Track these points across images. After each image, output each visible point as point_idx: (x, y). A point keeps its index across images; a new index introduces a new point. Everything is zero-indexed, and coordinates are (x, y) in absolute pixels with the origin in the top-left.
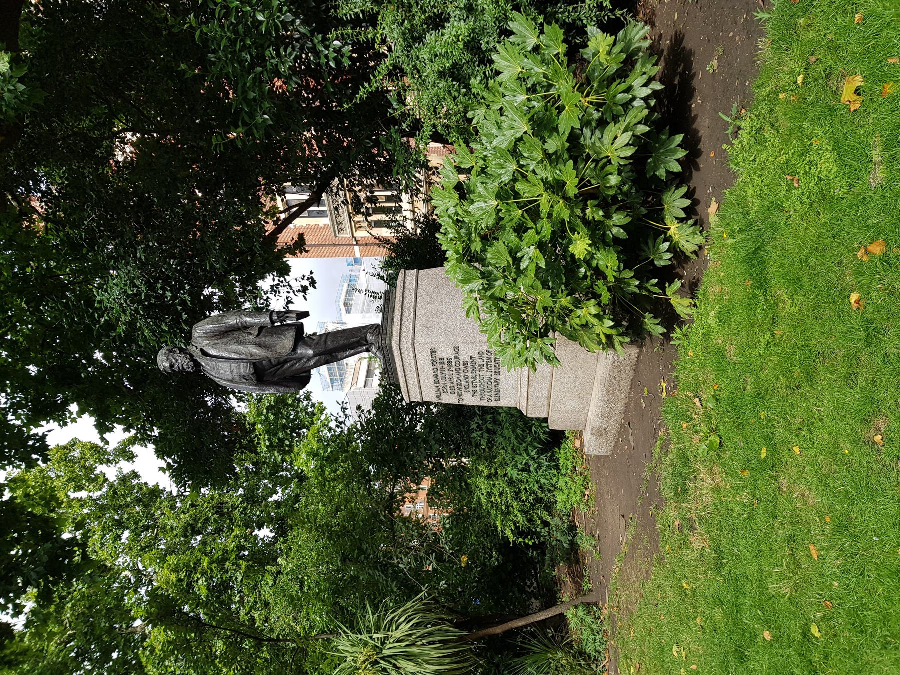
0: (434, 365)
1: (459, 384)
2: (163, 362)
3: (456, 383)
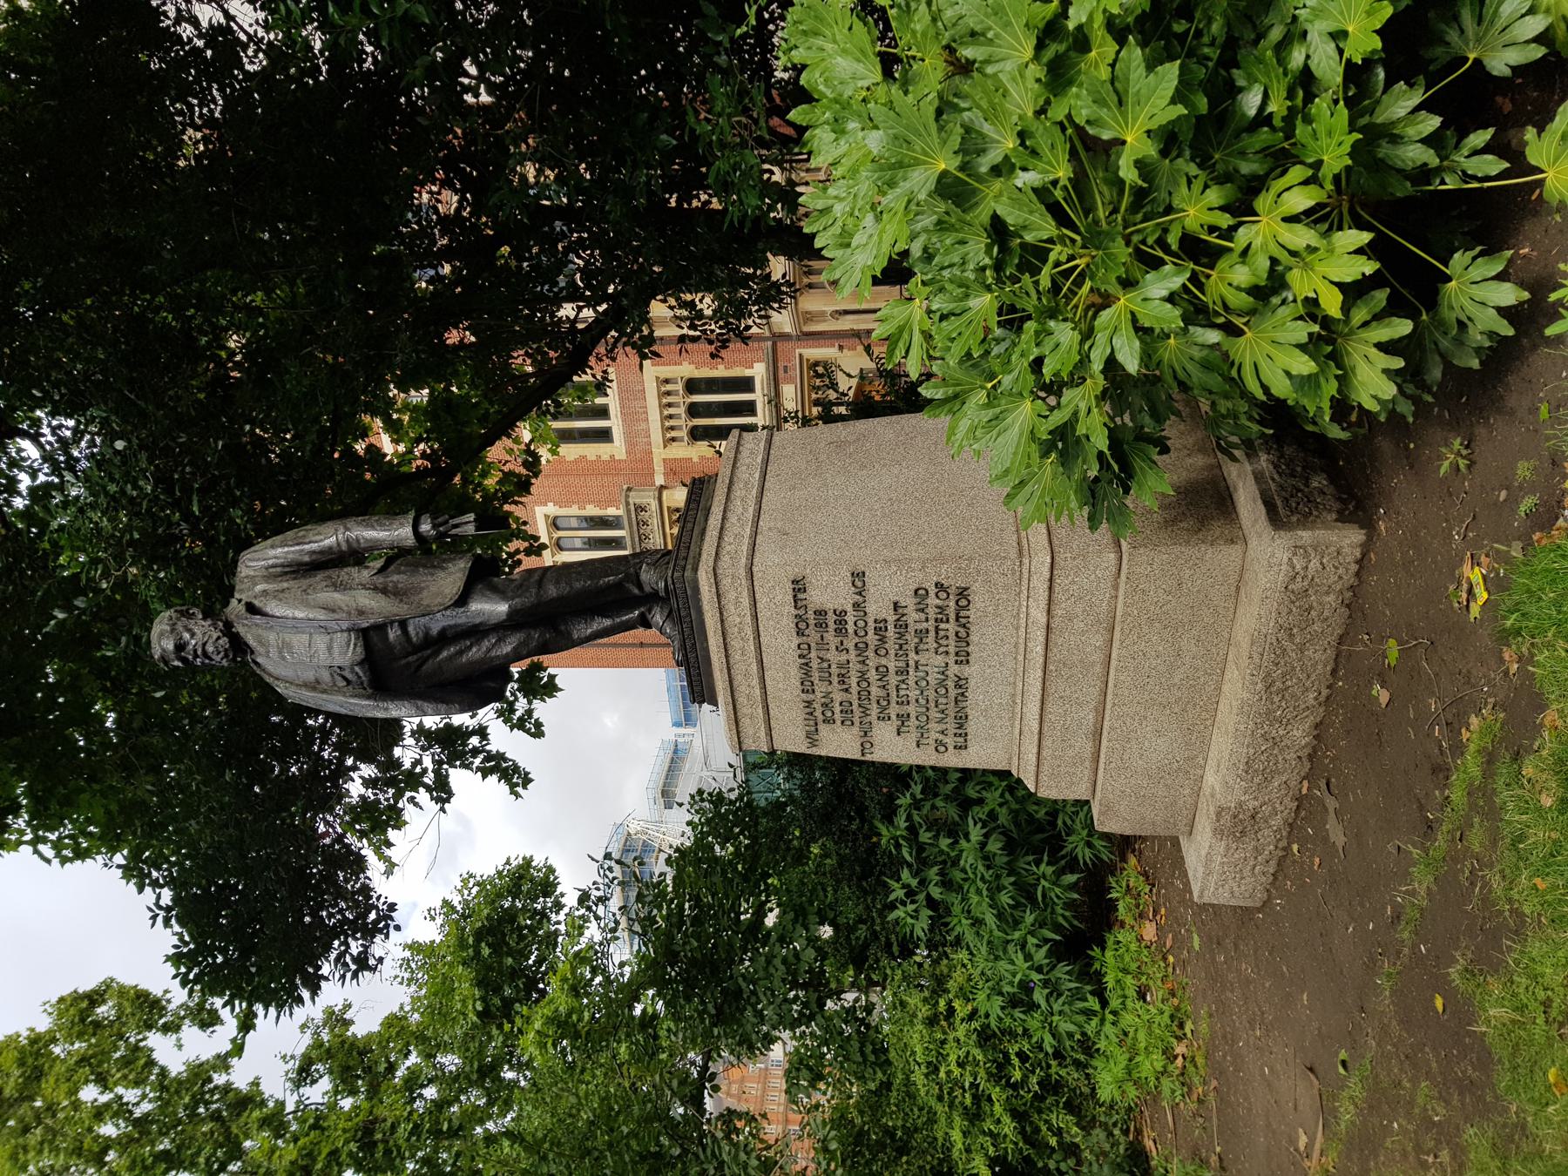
0: (800, 633)
1: (864, 695)
2: (161, 641)
3: (854, 689)
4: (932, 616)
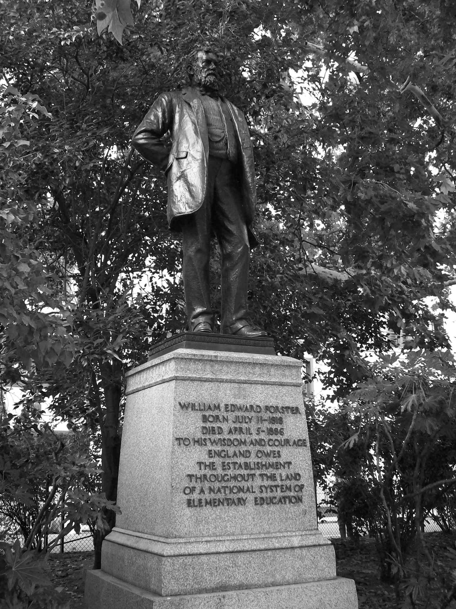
0: (267, 408)
1: (231, 443)
3: (232, 437)
4: (284, 483)
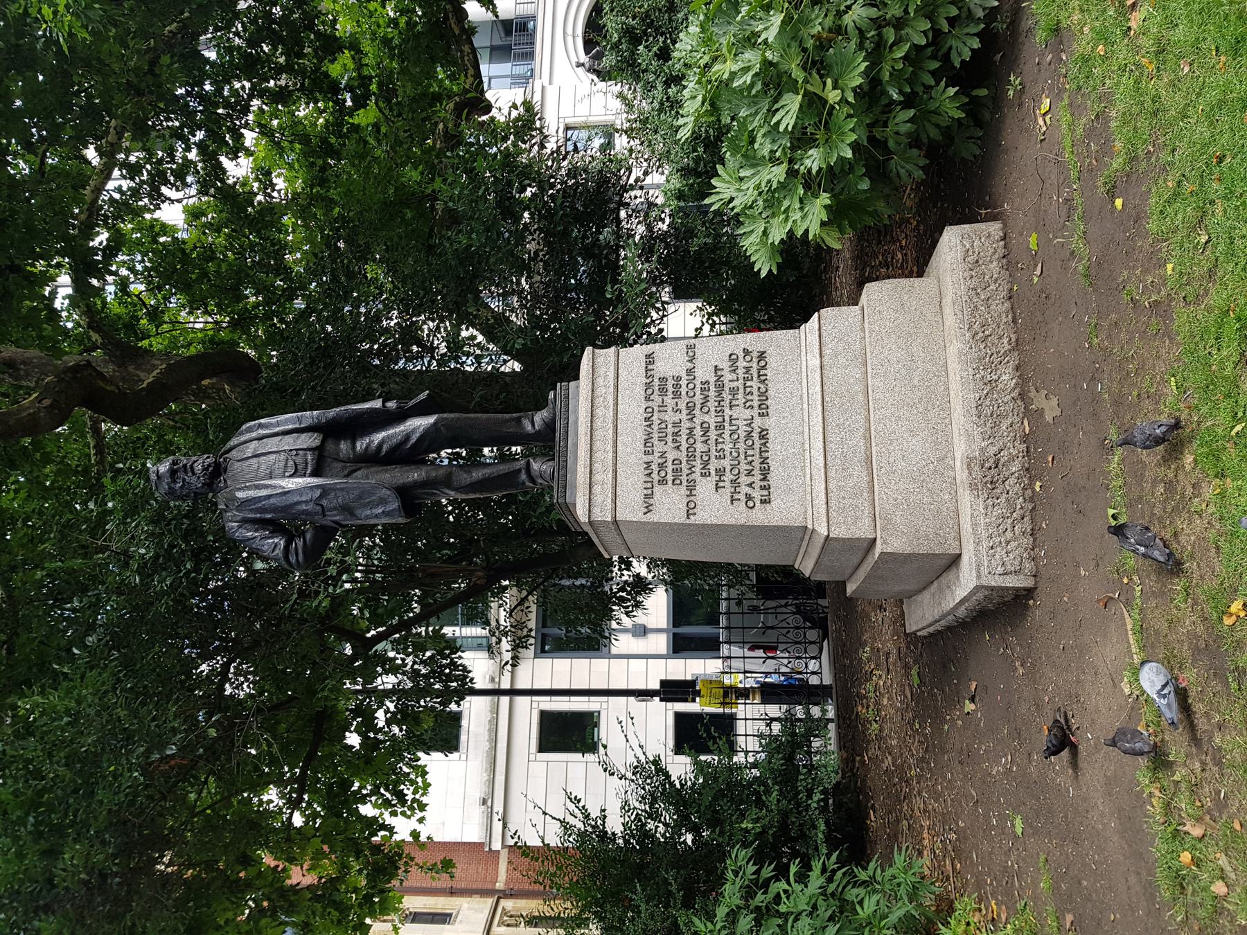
0: (647, 399)
3: (684, 445)
4: (741, 376)
